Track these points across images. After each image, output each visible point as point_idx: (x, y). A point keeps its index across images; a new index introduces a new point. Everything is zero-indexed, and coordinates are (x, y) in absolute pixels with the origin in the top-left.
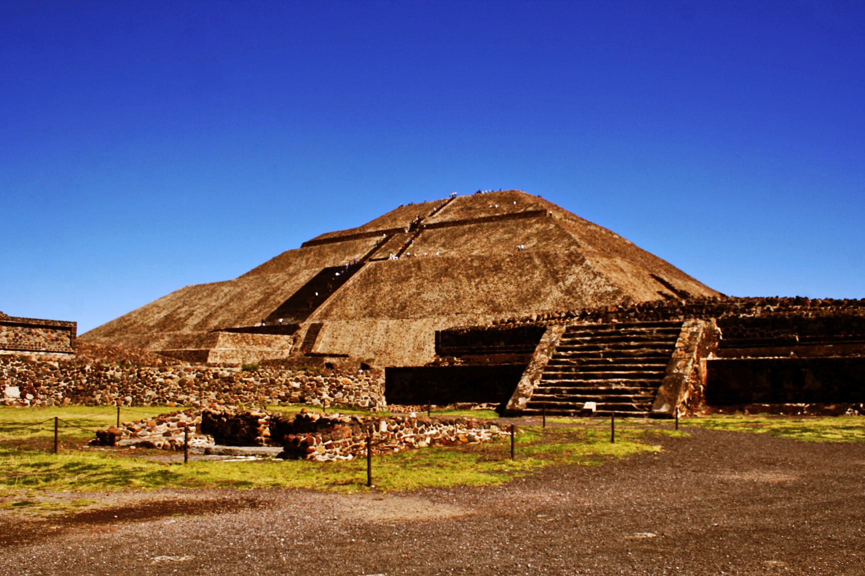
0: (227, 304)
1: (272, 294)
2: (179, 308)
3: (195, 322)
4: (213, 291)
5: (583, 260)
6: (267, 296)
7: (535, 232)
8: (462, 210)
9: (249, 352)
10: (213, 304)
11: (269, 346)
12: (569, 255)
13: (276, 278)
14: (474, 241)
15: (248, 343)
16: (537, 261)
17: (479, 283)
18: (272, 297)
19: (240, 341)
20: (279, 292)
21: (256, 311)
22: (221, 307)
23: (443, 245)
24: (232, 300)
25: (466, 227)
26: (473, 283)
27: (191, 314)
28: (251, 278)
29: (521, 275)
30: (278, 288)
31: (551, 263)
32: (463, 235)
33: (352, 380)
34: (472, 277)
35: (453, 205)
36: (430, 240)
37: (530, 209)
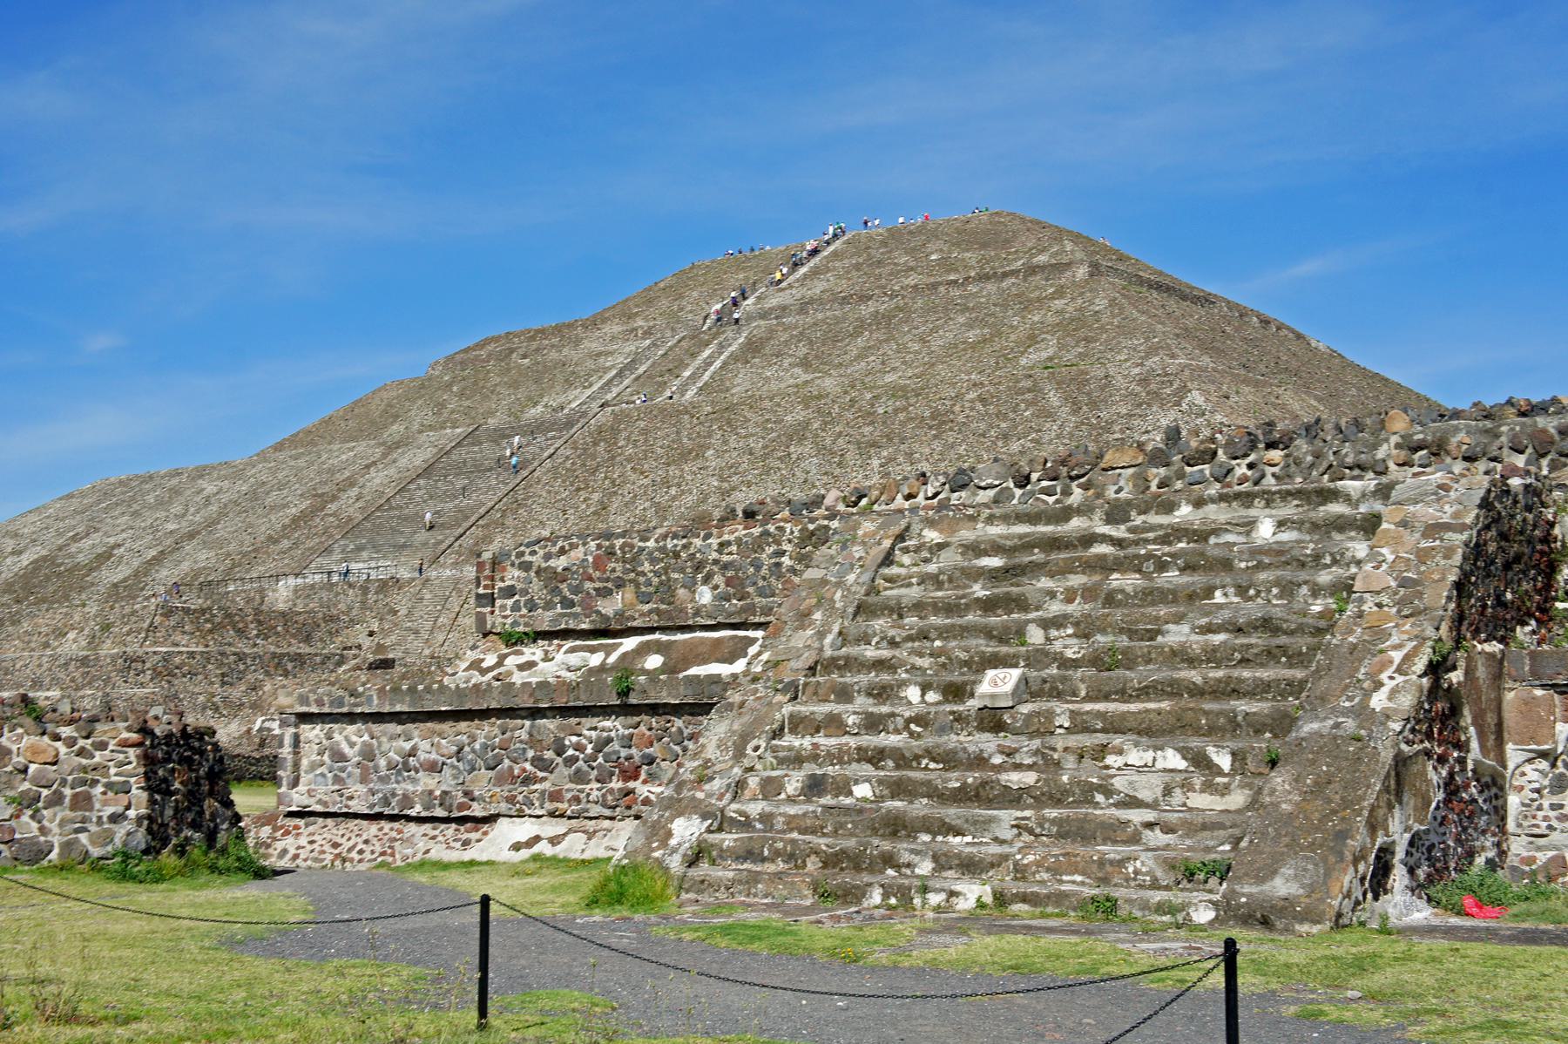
0: (212, 523)
1: (334, 498)
2: (75, 539)
3: (117, 577)
4: (175, 492)
5: (1184, 390)
6: (321, 501)
7: (1051, 319)
8: (857, 267)
9: (241, 657)
10: (171, 526)
11: (307, 639)
12: (1144, 381)
13: (342, 455)
14: (890, 349)
15: (241, 632)
16: (1054, 398)
17: (890, 460)
18: (332, 507)
19: (221, 626)
20: (354, 492)
21: (286, 543)
22: (191, 536)
23: (805, 364)
24: (222, 514)
25: (867, 309)
26: (876, 463)
27: (105, 557)
28: (281, 456)
29: (1005, 437)
30: (350, 482)
31: (1093, 405)
32: (857, 333)
33: (71, 742)
34: (874, 444)
35: (835, 254)
36: (767, 351)
37: (1042, 259)
